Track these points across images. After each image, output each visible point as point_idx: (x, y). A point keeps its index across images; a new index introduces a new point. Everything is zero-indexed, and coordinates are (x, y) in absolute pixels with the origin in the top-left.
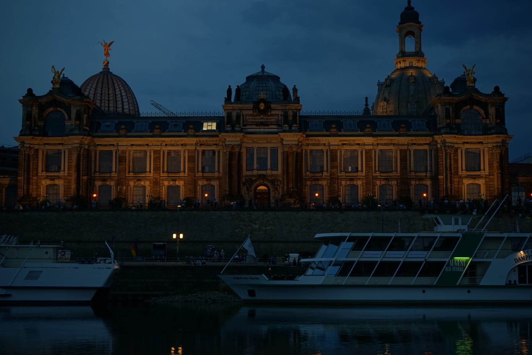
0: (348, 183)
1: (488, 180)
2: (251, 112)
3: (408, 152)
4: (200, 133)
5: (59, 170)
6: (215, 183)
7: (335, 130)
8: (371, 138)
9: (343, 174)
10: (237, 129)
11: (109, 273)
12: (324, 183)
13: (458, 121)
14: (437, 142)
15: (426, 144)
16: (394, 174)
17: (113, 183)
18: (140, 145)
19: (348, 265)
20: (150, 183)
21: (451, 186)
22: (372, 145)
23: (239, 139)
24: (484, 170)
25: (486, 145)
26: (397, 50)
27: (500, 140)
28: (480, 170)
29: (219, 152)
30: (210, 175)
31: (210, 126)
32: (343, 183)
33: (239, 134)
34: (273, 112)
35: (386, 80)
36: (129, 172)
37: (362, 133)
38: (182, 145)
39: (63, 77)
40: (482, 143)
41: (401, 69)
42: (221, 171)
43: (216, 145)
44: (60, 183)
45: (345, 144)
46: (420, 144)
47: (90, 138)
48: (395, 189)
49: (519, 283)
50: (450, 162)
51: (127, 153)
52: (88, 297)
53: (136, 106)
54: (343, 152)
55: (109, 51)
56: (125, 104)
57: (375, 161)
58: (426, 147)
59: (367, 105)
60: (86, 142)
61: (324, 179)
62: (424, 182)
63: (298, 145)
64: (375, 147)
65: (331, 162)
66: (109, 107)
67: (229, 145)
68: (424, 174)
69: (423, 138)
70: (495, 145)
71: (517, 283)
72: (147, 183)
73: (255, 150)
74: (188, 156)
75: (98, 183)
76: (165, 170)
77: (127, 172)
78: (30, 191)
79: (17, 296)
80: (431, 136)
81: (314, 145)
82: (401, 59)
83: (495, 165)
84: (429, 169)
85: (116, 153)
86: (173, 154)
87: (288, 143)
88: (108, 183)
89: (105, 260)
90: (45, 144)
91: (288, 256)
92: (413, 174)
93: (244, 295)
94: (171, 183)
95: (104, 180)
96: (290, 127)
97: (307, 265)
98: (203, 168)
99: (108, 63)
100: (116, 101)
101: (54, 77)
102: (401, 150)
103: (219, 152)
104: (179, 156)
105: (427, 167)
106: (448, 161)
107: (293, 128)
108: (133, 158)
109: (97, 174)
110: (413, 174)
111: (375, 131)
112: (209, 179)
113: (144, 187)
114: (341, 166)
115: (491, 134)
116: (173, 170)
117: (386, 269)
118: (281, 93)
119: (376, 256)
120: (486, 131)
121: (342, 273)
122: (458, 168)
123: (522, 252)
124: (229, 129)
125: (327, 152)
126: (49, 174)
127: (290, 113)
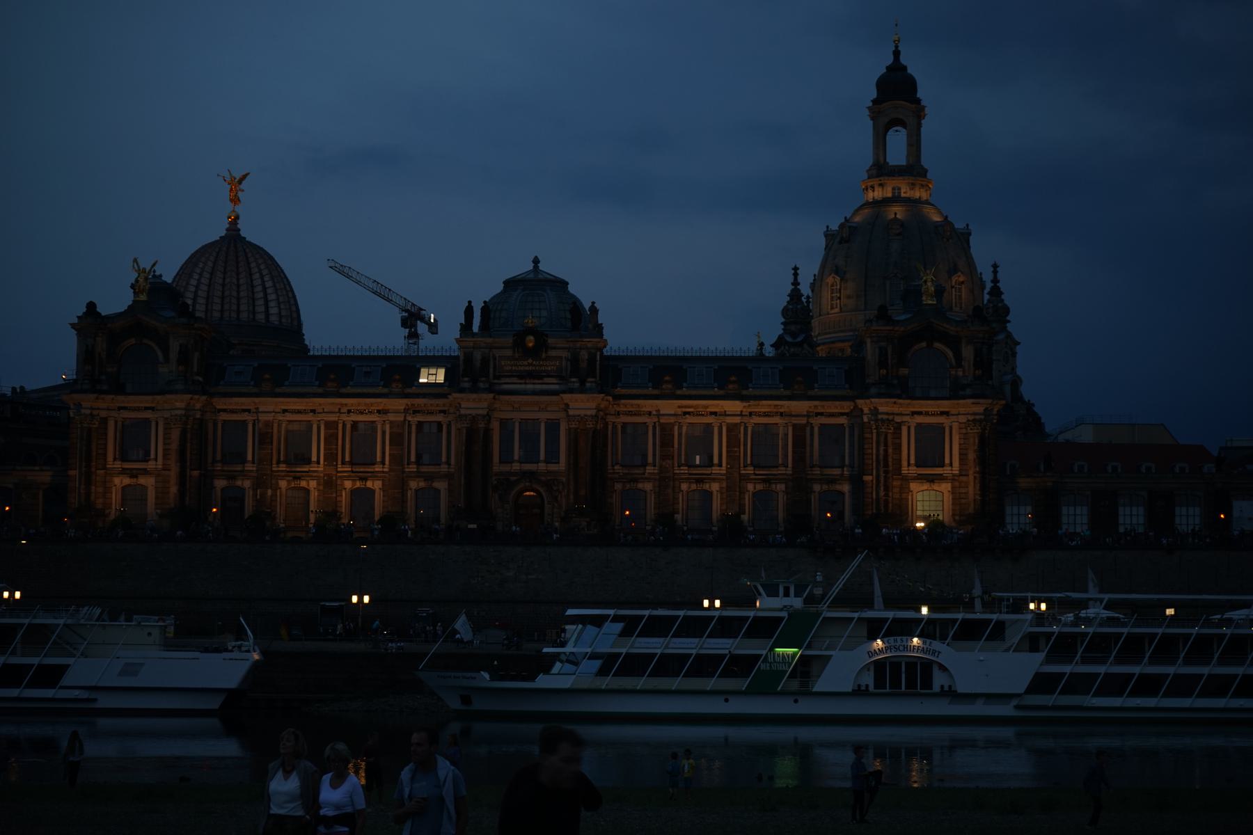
0: (694, 486)
1: (957, 484)
2: (509, 353)
3: (808, 429)
4: (413, 390)
5: (146, 459)
6: (441, 485)
7: (670, 386)
8: (738, 402)
9: (684, 470)
10: (481, 385)
11: (246, 666)
12: (648, 486)
13: (904, 371)
14: (862, 410)
15: (842, 414)
16: (782, 470)
17: (247, 484)
18: (299, 412)
19: (612, 657)
20: (318, 484)
21: (886, 495)
22: (741, 415)
23: (485, 405)
24: (951, 465)
25: (957, 419)
26: (867, 158)
27: (980, 409)
28: (942, 465)
29: (449, 425)
30: (432, 469)
31: (431, 376)
32: (684, 486)
33: (484, 396)
34: (553, 353)
35: (842, 226)
36: (279, 462)
37: (722, 392)
38: (379, 412)
39: (154, 276)
40: (946, 413)
41: (876, 203)
42: (453, 461)
43: (444, 412)
44: (148, 482)
45: (689, 413)
46: (832, 415)
47: (204, 398)
48: (782, 499)
49: (875, 688)
50: (886, 451)
51: (275, 425)
52: (214, 703)
53: (294, 308)
54: (684, 429)
55: (240, 194)
56: (272, 304)
57: (745, 445)
58: (842, 420)
59: (796, 283)
60: (198, 406)
61: (648, 479)
62: (838, 487)
63: (596, 416)
64: (745, 420)
65: (662, 446)
66: (238, 312)
67: (466, 416)
68: (837, 472)
69: (837, 403)
70: (971, 418)
71: (871, 688)
72: (313, 484)
73: (517, 425)
74: (391, 434)
75: (220, 483)
76: (347, 459)
77: (274, 462)
78: (92, 498)
79: (105, 702)
80: (852, 399)
81: (630, 414)
82: (875, 182)
83: (972, 456)
84: (847, 462)
85: (254, 425)
86: (361, 426)
87: (577, 413)
88: (239, 483)
89: (240, 647)
90: (120, 408)
91: (564, 631)
92: (817, 471)
93: (455, 704)
94: (358, 484)
95: (231, 477)
96: (583, 382)
97: (555, 657)
98: (419, 457)
99: (237, 218)
100: (254, 300)
101: (137, 281)
102: (794, 426)
103: (449, 425)
104: (375, 430)
105: (843, 457)
106: (882, 448)
107: (588, 385)
108: (287, 431)
109: (219, 467)
110: (817, 471)
111: (747, 388)
112: (429, 478)
113: (307, 491)
114: (679, 455)
115: (964, 398)
116: (362, 459)
117: (668, 665)
118: (569, 316)
119: (654, 646)
120: (956, 392)
121: (603, 672)
122: (900, 460)
123: (879, 641)
124: (466, 385)
125: (654, 427)
126: (127, 465)
127: (584, 355)
